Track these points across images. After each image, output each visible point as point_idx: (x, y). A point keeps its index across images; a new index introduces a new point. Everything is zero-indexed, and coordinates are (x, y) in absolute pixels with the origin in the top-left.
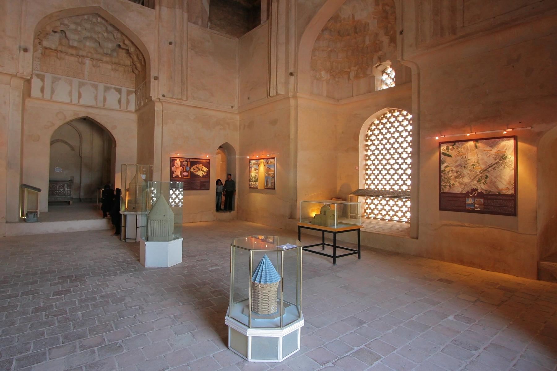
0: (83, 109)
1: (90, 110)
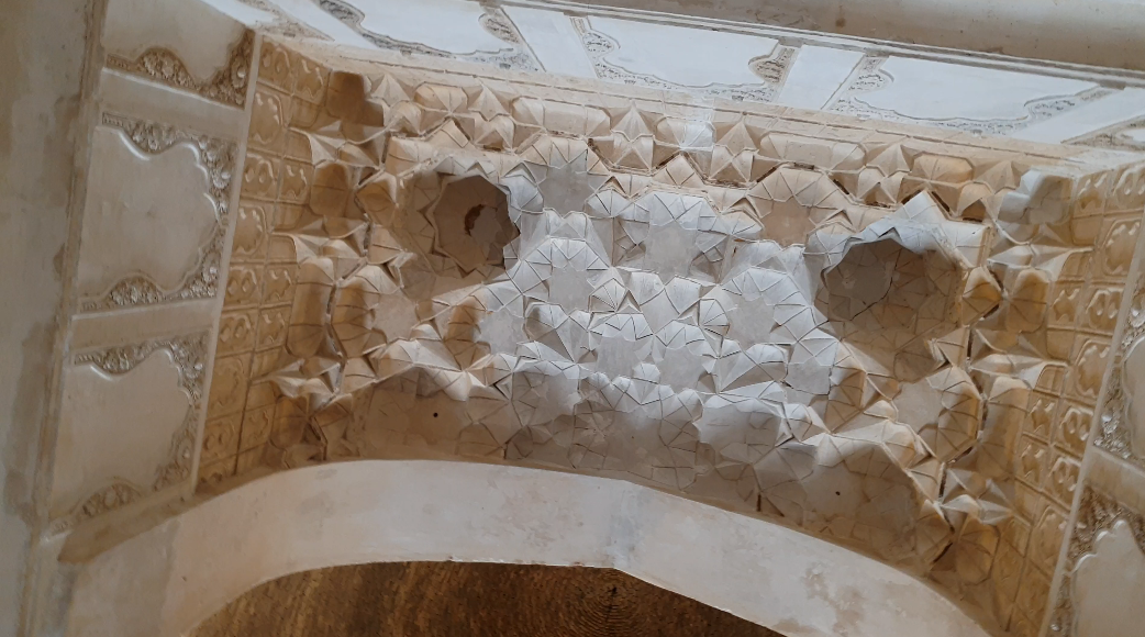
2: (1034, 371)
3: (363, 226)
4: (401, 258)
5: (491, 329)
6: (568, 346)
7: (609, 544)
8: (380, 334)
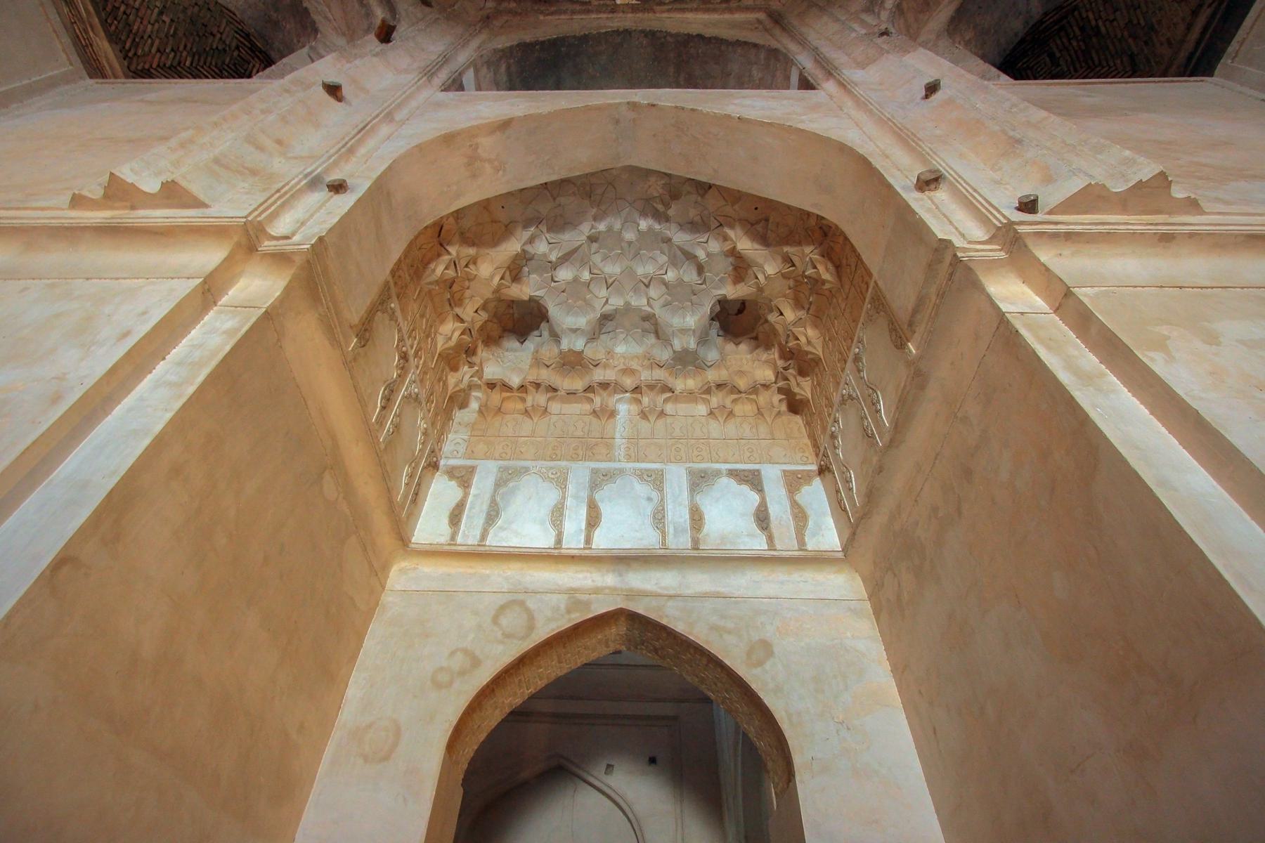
0: (607, 579)
1: (639, 580)
2: (440, 344)
3: (790, 344)
4: (772, 318)
5: (725, 265)
6: (679, 253)
7: (634, 120)
8: (785, 276)
